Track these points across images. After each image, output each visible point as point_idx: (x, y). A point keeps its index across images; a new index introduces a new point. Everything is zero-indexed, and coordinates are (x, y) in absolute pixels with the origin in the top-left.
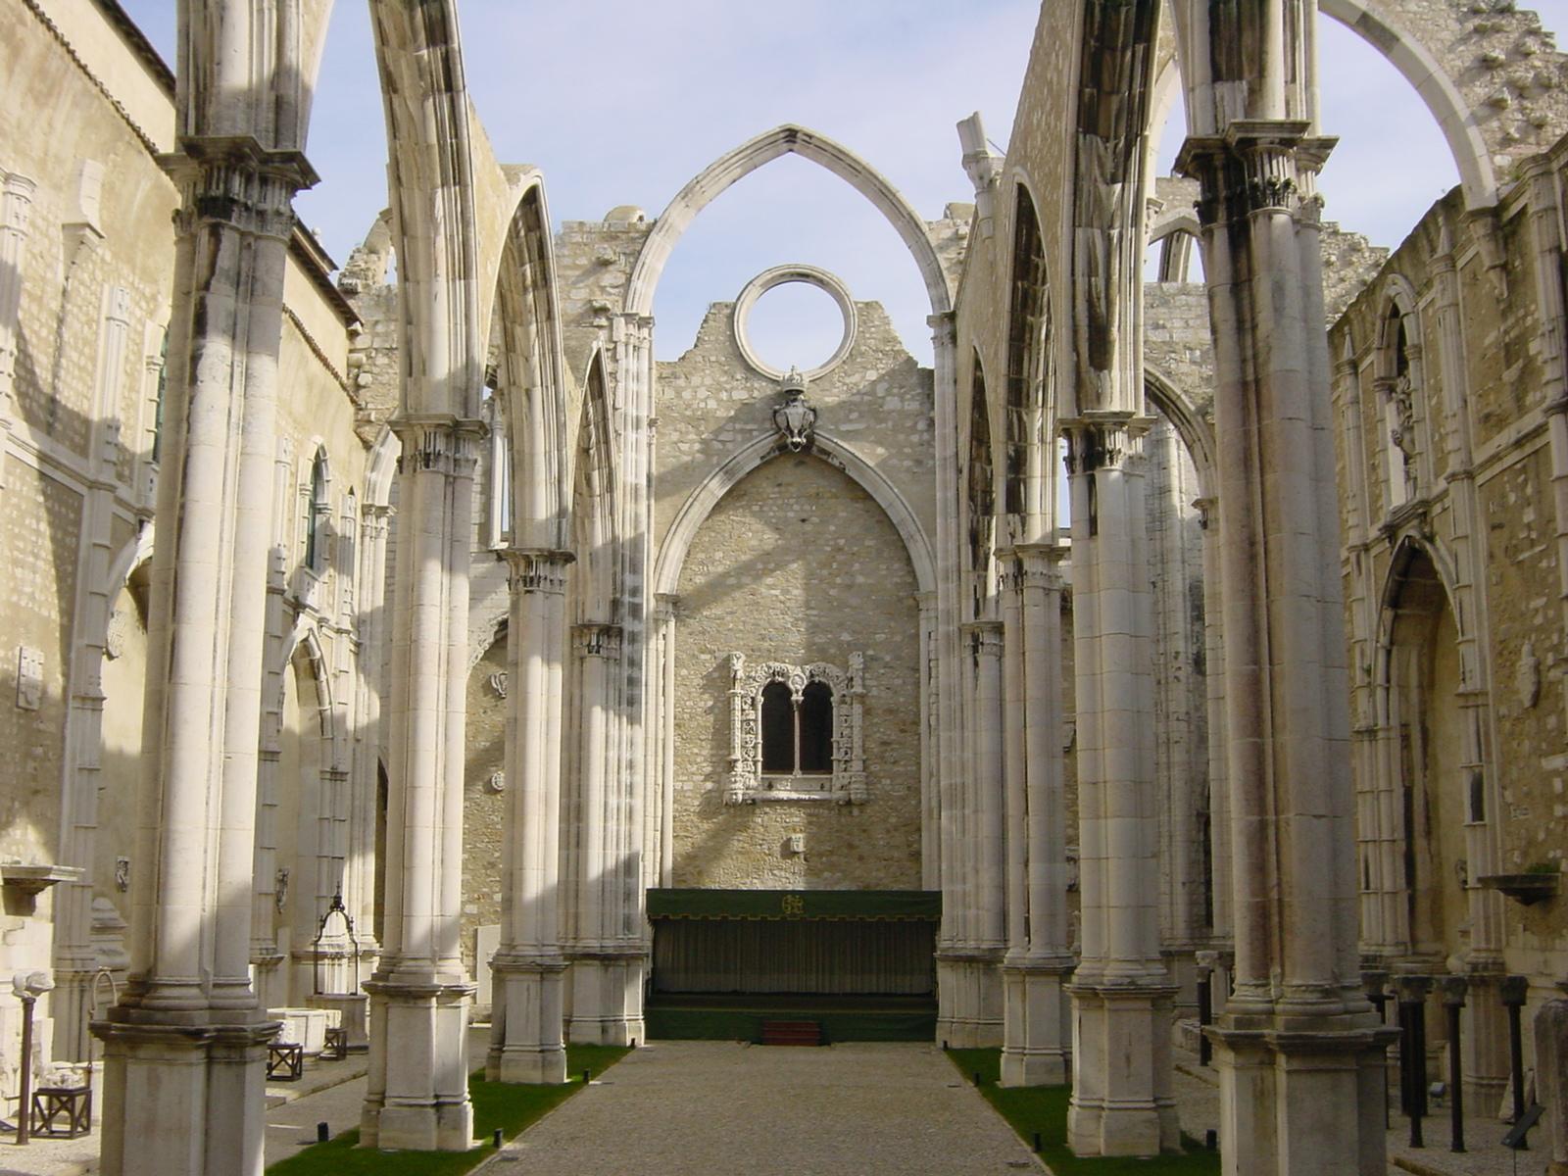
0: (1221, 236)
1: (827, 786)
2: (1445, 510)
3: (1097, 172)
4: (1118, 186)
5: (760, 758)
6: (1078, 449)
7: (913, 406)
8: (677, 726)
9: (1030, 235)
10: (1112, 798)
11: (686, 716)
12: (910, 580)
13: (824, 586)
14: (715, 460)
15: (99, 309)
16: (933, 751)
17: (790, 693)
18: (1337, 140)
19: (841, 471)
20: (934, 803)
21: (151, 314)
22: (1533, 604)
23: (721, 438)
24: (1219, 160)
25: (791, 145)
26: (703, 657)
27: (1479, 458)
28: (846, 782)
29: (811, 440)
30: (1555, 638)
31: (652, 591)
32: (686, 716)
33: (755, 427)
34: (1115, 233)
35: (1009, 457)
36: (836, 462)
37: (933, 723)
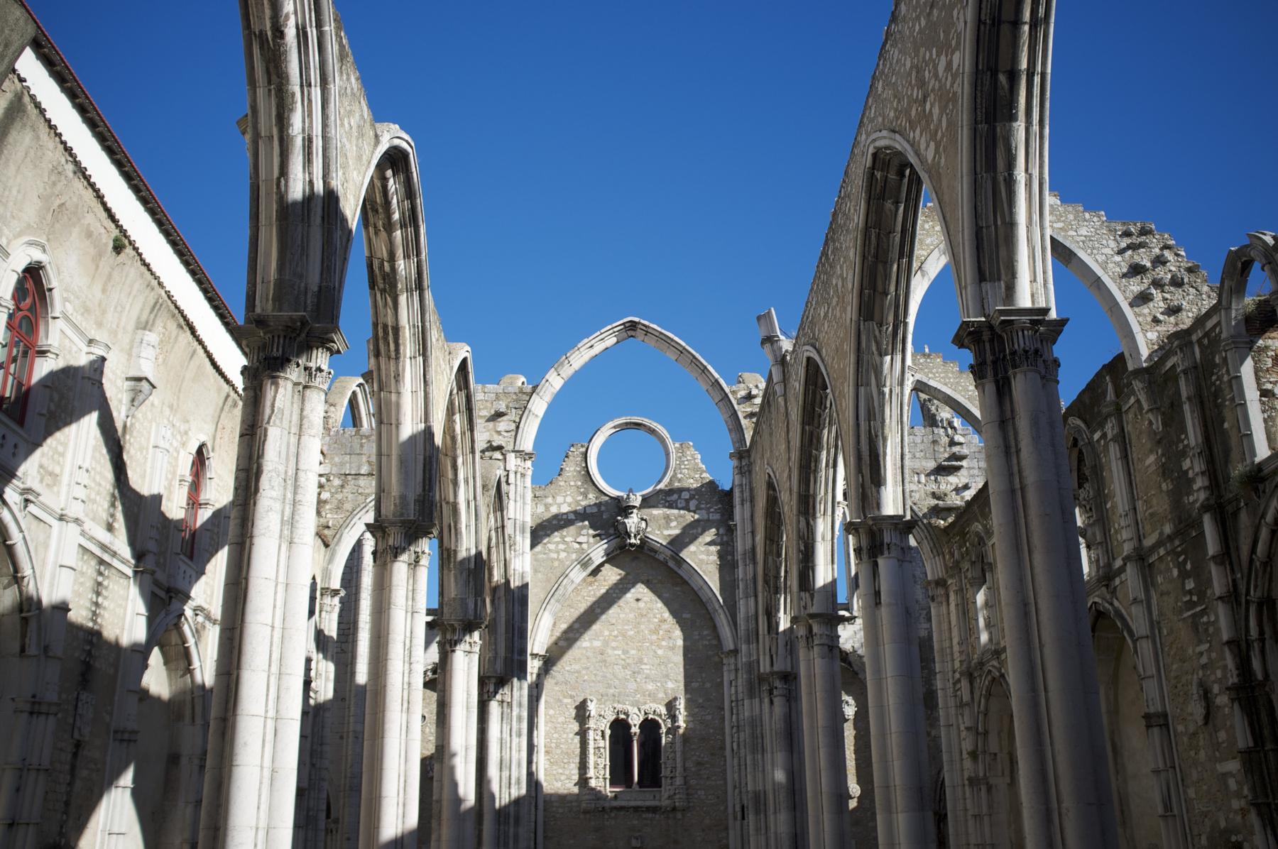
0: (990, 387)
2: (1122, 582)
3: (874, 348)
4: (888, 358)
5: (608, 776)
6: (864, 544)
7: (717, 517)
8: (547, 752)
9: (814, 393)
10: (900, 798)
12: (715, 642)
14: (574, 556)
15: (149, 439)
16: (736, 768)
17: (629, 727)
18: (1067, 320)
19: (665, 564)
20: (738, 808)
21: (184, 444)
22: (1198, 649)
24: (986, 336)
25: (630, 333)
26: (566, 701)
27: (1148, 542)
29: (644, 541)
30: (1219, 673)
34: (887, 390)
35: (799, 551)
36: (661, 557)
37: (735, 747)
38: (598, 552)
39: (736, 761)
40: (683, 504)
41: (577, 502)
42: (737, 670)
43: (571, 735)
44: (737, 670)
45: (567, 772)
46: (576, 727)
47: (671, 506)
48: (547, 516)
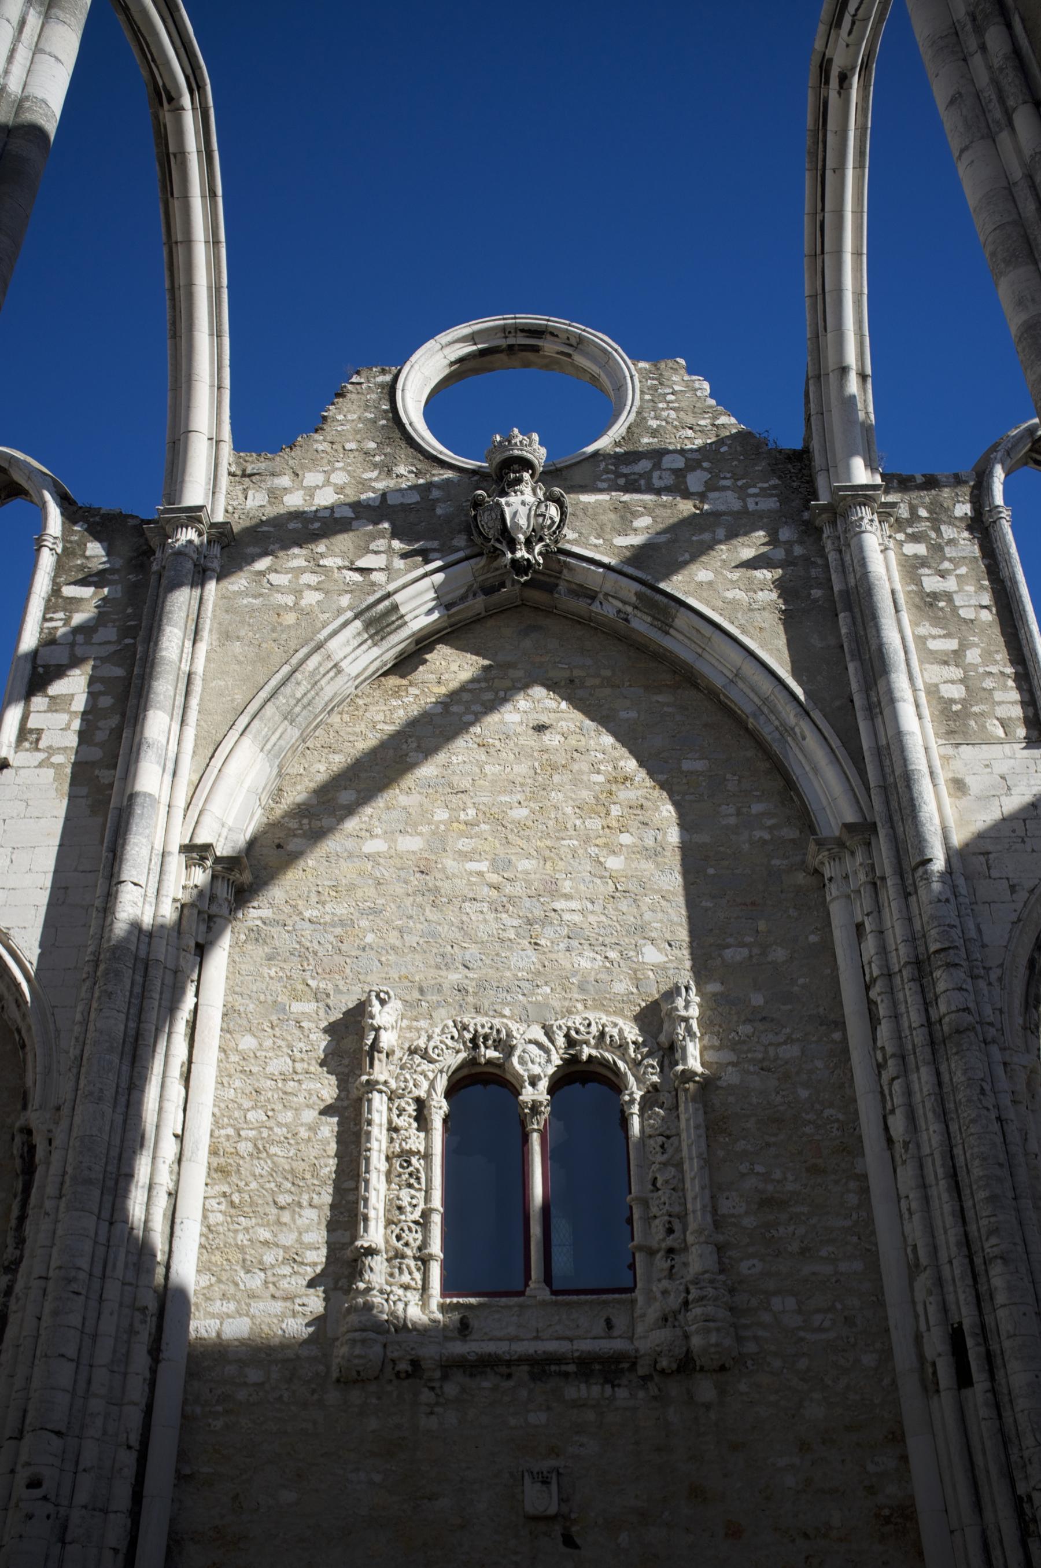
1: (621, 1323)
5: (436, 1247)
7: (770, 504)
11: (245, 1147)
12: (790, 833)
13: (593, 850)
14: (345, 600)
20: (936, 1344)
23: (360, 564)
26: (297, 1007)
28: (674, 1301)
31: (179, 837)
32: (245, 1147)
33: (435, 544)
36: (608, 610)
37: (898, 1125)
38: (418, 597)
39: (907, 1175)
40: (669, 480)
41: (364, 485)
42: (875, 885)
43: (310, 1115)
44: (875, 885)
45: (288, 1239)
46: (327, 1089)
47: (631, 486)
48: (271, 512)
